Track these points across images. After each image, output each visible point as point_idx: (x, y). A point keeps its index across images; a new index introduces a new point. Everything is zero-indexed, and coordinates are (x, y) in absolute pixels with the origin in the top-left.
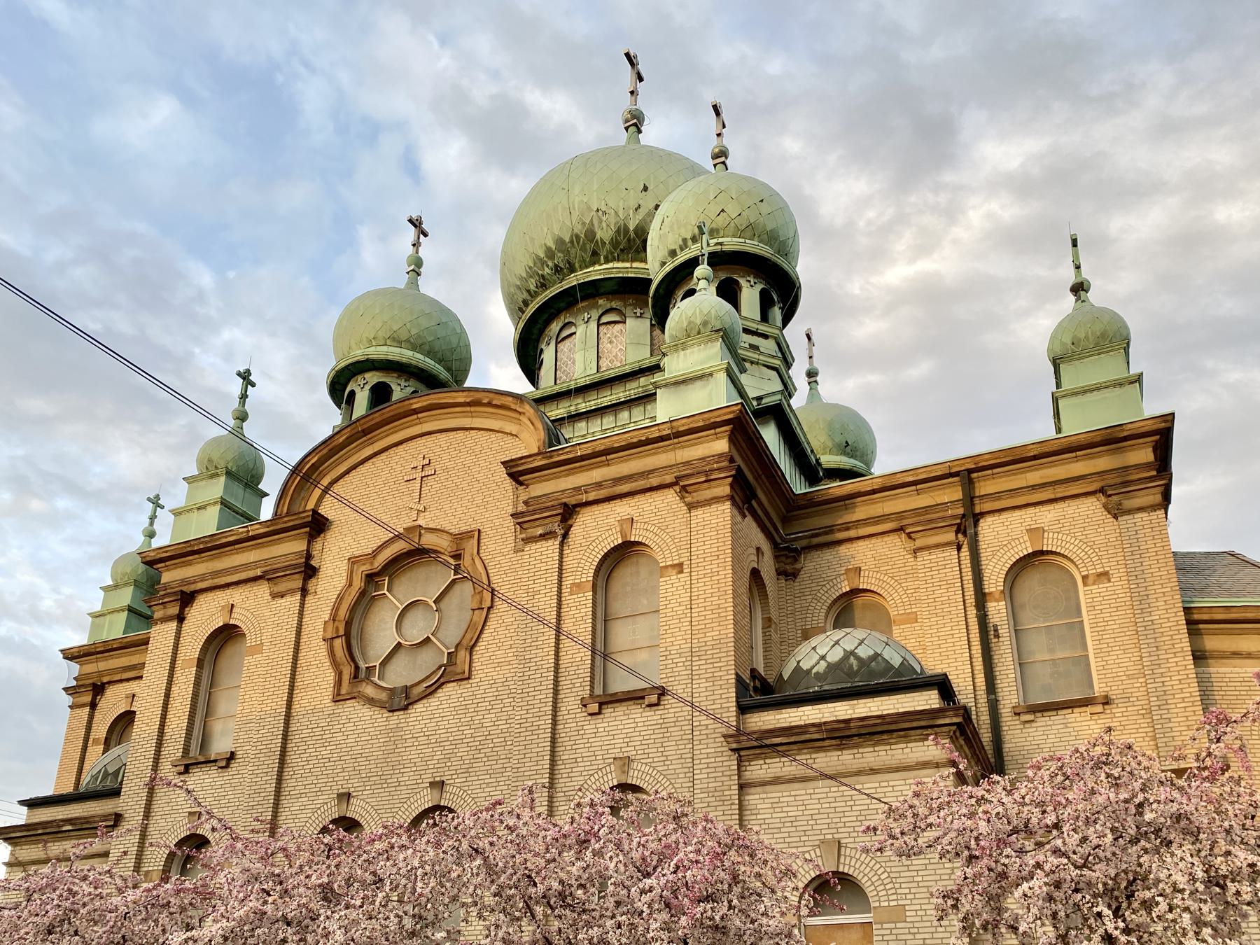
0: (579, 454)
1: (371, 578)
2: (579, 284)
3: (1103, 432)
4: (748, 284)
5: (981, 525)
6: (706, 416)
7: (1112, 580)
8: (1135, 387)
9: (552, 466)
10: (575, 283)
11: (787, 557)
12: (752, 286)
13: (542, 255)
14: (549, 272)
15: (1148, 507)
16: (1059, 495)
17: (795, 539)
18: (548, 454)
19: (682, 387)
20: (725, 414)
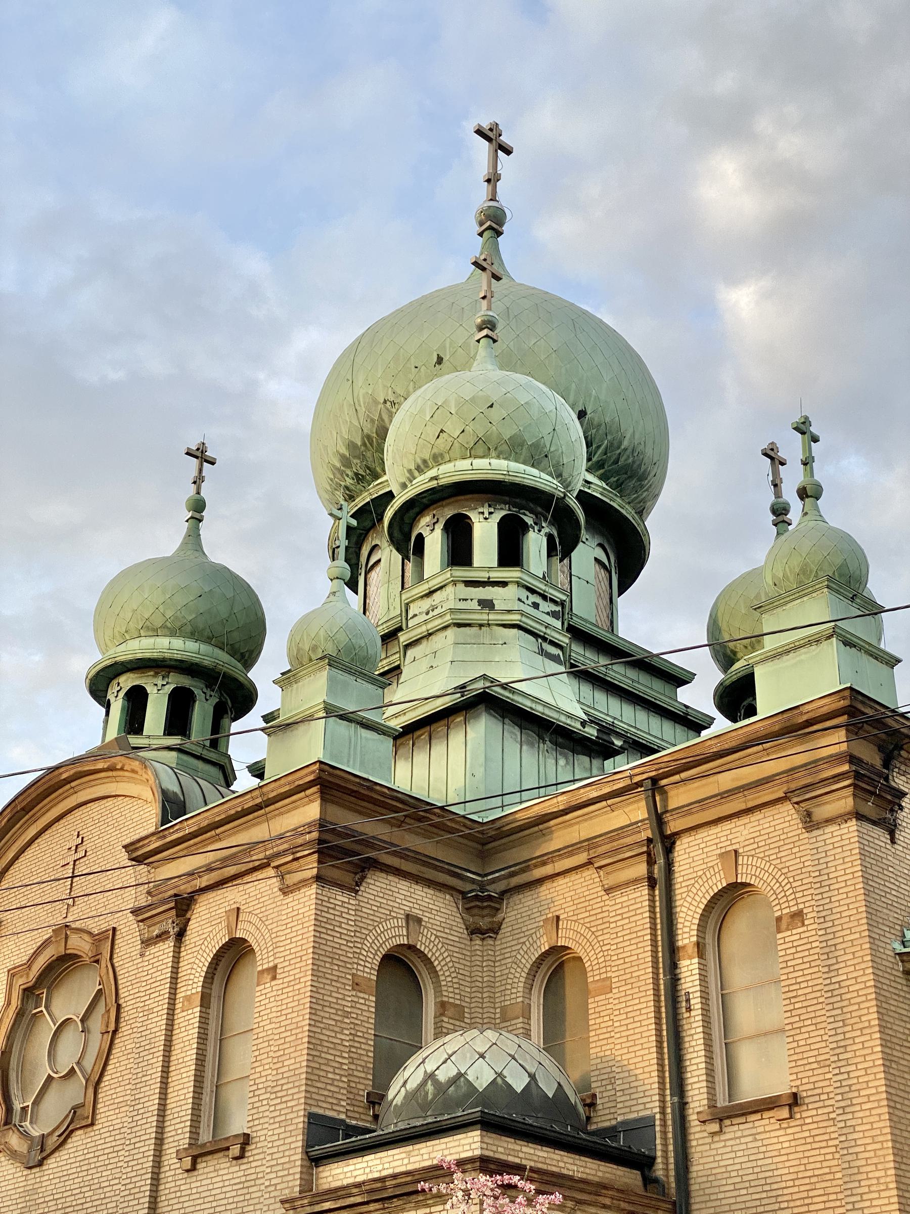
0: (187, 832)
1: (28, 992)
2: (372, 500)
3: (780, 717)
4: (481, 516)
5: (677, 849)
6: (290, 778)
7: (806, 922)
8: (832, 643)
9: (168, 846)
10: (368, 500)
11: (483, 908)
12: (486, 519)
13: (338, 465)
14: (351, 481)
15: (840, 816)
16: (750, 804)
17: (493, 881)
18: (161, 834)
19: (289, 733)
20: (306, 775)
